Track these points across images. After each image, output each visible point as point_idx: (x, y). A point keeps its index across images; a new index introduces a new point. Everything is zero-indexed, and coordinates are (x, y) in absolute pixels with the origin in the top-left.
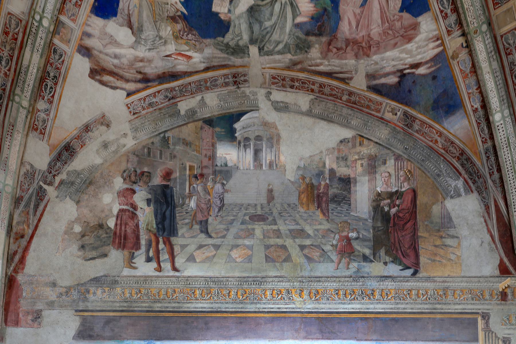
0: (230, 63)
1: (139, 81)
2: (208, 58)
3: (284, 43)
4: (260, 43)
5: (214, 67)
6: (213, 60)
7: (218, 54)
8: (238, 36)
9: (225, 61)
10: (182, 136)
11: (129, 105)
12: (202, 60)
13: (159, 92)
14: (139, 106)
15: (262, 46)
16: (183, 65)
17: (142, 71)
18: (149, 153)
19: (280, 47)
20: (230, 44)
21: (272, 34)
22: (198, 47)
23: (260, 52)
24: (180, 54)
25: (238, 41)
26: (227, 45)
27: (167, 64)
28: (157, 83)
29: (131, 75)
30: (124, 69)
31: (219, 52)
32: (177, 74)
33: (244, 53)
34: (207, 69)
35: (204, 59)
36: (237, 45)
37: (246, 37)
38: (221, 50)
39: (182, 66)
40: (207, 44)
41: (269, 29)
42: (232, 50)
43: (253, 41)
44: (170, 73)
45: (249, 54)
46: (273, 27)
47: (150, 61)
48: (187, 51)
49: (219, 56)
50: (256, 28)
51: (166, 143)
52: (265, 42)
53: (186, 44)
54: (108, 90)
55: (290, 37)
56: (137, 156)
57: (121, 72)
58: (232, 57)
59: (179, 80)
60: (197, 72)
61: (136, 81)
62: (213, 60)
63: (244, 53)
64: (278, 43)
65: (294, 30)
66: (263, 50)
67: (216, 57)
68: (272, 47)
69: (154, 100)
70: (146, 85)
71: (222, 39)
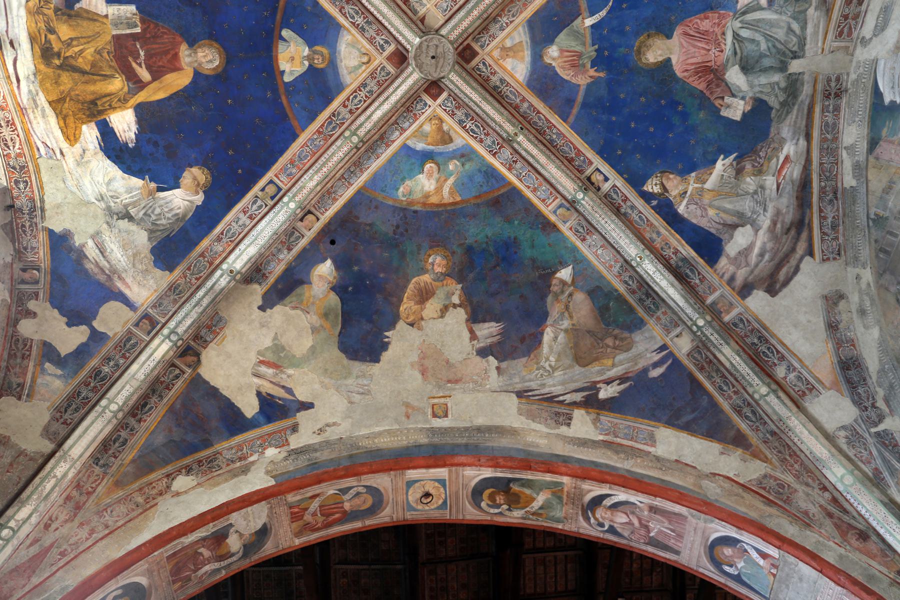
0: (807, 103)
1: (799, 233)
2: (794, 133)
3: (791, 20)
4: (786, 57)
5: (807, 126)
6: (798, 125)
7: (792, 118)
8: (773, 89)
9: (803, 109)
10: (879, 193)
11: (825, 257)
12: (794, 141)
13: (821, 211)
14: (830, 244)
15: (791, 55)
16: (793, 170)
17: (788, 227)
18: (886, 252)
19: (795, 26)
20: (781, 99)
21: (777, 39)
22: (776, 145)
23: (799, 57)
24: (780, 171)
25: (779, 88)
26: (783, 104)
27: (787, 190)
28: (808, 211)
29: (788, 243)
30: (778, 249)
31: (790, 116)
32: (803, 181)
33: (797, 80)
34: (808, 137)
35: (793, 139)
36: (785, 90)
37: (777, 77)
38: (788, 113)
39: (795, 172)
40: (776, 132)
41: (770, 45)
42: (790, 98)
43: (783, 67)
44: (800, 190)
45: (800, 74)
46: (768, 37)
47: (778, 213)
48: (778, 160)
49: (794, 117)
50: (767, 62)
51: (880, 220)
52: (786, 50)
53: (770, 160)
54: (798, 278)
55: (785, 13)
56: (884, 272)
57: (781, 254)
58: (800, 99)
59: (812, 179)
60: (808, 151)
61: (797, 239)
62: (798, 125)
63: (797, 80)
64: (790, 30)
65: (775, 7)
66: (796, 52)
67: (795, 122)
68: (795, 39)
69: (830, 220)
70: (806, 227)
71: (774, 111)
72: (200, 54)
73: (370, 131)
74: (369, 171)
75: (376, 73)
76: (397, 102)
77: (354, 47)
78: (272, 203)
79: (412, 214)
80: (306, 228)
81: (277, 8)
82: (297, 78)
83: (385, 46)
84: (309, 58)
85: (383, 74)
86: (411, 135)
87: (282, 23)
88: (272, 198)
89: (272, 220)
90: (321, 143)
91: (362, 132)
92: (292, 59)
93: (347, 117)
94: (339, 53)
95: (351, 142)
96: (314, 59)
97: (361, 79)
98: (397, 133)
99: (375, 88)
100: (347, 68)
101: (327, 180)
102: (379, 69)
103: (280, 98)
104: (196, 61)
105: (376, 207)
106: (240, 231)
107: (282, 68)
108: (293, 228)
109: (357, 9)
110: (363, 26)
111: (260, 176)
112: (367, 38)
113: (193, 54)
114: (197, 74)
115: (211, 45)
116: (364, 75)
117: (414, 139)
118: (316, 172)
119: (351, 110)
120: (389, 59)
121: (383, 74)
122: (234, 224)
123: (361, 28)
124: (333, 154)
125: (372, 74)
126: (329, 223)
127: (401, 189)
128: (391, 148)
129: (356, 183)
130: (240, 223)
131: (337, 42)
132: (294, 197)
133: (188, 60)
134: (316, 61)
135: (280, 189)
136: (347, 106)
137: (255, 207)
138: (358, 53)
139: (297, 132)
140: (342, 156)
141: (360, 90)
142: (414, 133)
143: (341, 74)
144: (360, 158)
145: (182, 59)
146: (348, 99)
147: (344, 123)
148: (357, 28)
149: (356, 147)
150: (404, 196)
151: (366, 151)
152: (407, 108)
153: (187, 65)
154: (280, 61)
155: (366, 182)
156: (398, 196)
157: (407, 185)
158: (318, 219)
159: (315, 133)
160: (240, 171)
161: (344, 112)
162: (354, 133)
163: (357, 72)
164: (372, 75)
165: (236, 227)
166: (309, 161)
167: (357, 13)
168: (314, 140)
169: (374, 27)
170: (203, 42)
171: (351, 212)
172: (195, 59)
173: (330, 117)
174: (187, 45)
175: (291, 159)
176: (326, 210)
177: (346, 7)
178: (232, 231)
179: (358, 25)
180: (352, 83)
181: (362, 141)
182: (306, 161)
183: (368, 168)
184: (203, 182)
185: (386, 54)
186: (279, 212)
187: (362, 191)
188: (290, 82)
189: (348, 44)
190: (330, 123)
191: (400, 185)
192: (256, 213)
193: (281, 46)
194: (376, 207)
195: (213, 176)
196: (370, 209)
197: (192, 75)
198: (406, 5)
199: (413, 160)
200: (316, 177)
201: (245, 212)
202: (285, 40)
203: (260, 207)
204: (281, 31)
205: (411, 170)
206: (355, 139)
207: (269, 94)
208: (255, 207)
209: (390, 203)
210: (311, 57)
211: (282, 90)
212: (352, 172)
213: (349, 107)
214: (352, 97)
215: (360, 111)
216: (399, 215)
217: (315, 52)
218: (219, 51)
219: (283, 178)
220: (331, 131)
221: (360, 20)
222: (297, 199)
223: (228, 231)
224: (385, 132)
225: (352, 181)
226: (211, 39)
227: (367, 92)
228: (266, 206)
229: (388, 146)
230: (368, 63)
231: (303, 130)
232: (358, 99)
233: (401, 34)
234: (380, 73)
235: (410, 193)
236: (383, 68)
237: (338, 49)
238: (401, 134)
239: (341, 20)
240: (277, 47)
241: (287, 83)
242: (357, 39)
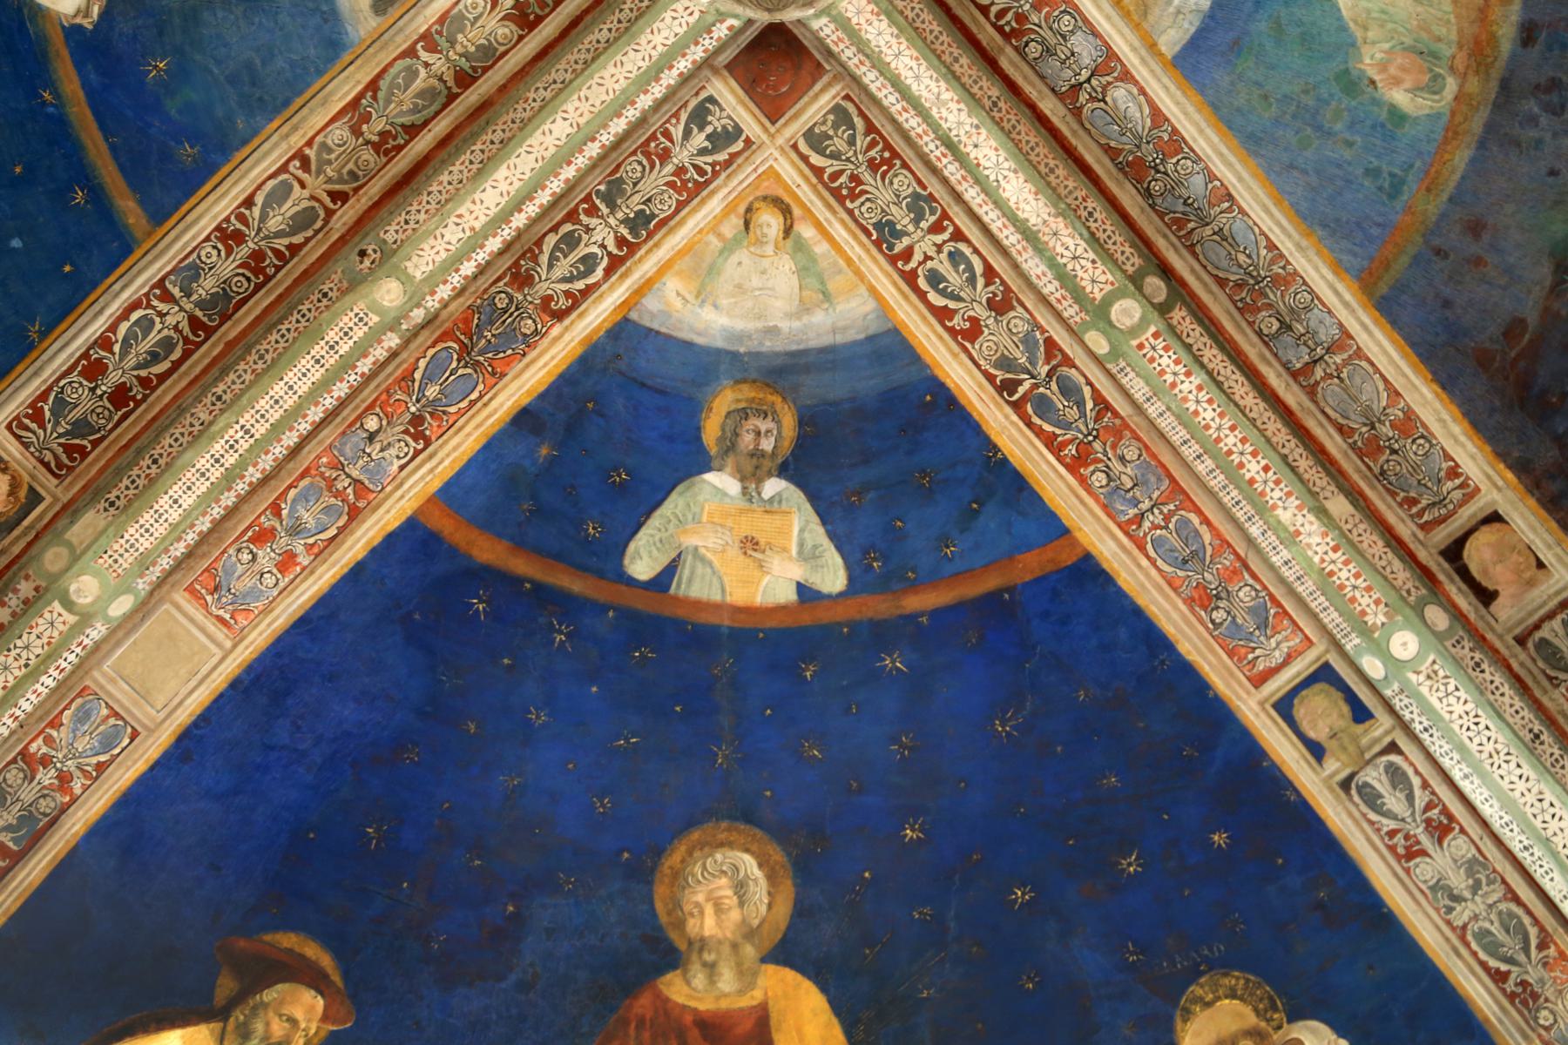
72: (708, 925)
73: (1093, 239)
74: (1286, 246)
75: (835, 176)
76: (972, 98)
77: (713, 270)
78: (1383, 721)
79: (1536, 51)
80: (1531, 583)
81: (539, 587)
82: (832, 536)
83: (715, 123)
84: (751, 476)
85: (839, 144)
86: (1137, 27)
87: (601, 574)
88: (1361, 714)
89: (1461, 748)
90: (1131, 453)
91: (1096, 277)
92: (750, 544)
93: (1021, 327)
94: (741, 337)
95: (1134, 331)
96: (757, 454)
97: (856, 248)
98: (1120, 95)
99: (903, 182)
100: (805, 308)
101: (1304, 463)
102: (816, 160)
103: (912, 618)
104: (735, 946)
105: (1475, 228)
106: (1497, 893)
107: (787, 595)
108: (1521, 641)
109: (551, 240)
110: (625, 221)
111: (1252, 753)
112: (681, 205)
113: (709, 957)
114: (784, 953)
115: (677, 875)
116: (839, 232)
117: (1156, 12)
118: (1262, 509)
119: (991, 304)
120: (773, 111)
121: (839, 144)
122: (1461, 915)
123: (636, 234)
124: (1186, 419)
125: (836, 193)
126: (1522, 468)
127: (1400, 97)
128: (1188, 130)
129: (1343, 314)
130: (1459, 882)
131: (688, 345)
132: (1365, 631)
133: (727, 981)
134: (767, 445)
135: (1323, 674)
136: (974, 321)
137: (1394, 801)
138: (742, 255)
139: (1068, 558)
140: (1196, 380)
141: (908, 254)
142: (1126, 15)
143: (827, 340)
144: (1222, 283)
145: (724, 1005)
146: (942, 314)
147: (1050, 343)
148: (632, 248)
149: (1163, 309)
150: (1433, 86)
151: (1191, 248)
152: (1007, 37)
153: (751, 986)
154: (759, 600)
155: (1338, 267)
156: (1434, 117)
157: (1383, 67)
158: (1494, 518)
159: (1083, 481)
160: (1219, 839)
161: (998, 337)
162: (1100, 313)
163: (824, 264)
164: (843, 193)
165: (1477, 905)
166: (1206, 521)
167: (571, 241)
168: (1115, 488)
169: (632, 169)
170: (659, 906)
171: (1483, 360)
172: (726, 949)
173: (1017, 406)
174: (669, 976)
175: (1190, 601)
176: (1454, 472)
177: (542, 289)
178: (1495, 929)
179: (621, 242)
180: (873, 291)
181: (1136, 280)
182: (1207, 537)
183: (1271, 246)
184: (1247, 1011)
185: (750, 122)
186: (1426, 709)
187: (1383, 289)
188: (849, 567)
189: (702, 296)
190: (1044, 406)
191: (1375, 102)
192: (1421, 799)
193: (696, 586)
194: (1475, 228)
195: (1225, 965)
196: (1478, 261)
197: (789, 975)
198: (539, 20)
199: (1261, 26)
200: (1285, 516)
201: (1414, 852)
202: (671, 570)
203: (1397, 777)
204: (631, 582)
205: (1307, 39)
206: (1127, 311)
207: (893, 662)
208: (1394, 801)
209: (1461, 158)
210: (748, 466)
211: (879, 607)
212: (1286, 327)
213: (981, 312)
214: (933, 297)
215: (998, 264)
216: (1533, 120)
217: (729, 445)
218: (702, 845)
219: (1273, 649)
220: (1080, 404)
221: (602, 234)
222: (1376, 617)
223: (1493, 948)
224: (1107, 149)
225: (1327, 333)
226: (653, 870)
227: (916, 221)
228: (1393, 748)
229: (1177, 143)
230: (786, 211)
231: (1059, 530)
232: (943, 265)
233: (666, 62)
234: (835, 156)
235: (1424, 53)
236: (815, 139)
237: (720, 343)
238: (1127, 76)
239: (595, 316)
240: (698, 605)
241: (851, 579)
242: (681, 253)
